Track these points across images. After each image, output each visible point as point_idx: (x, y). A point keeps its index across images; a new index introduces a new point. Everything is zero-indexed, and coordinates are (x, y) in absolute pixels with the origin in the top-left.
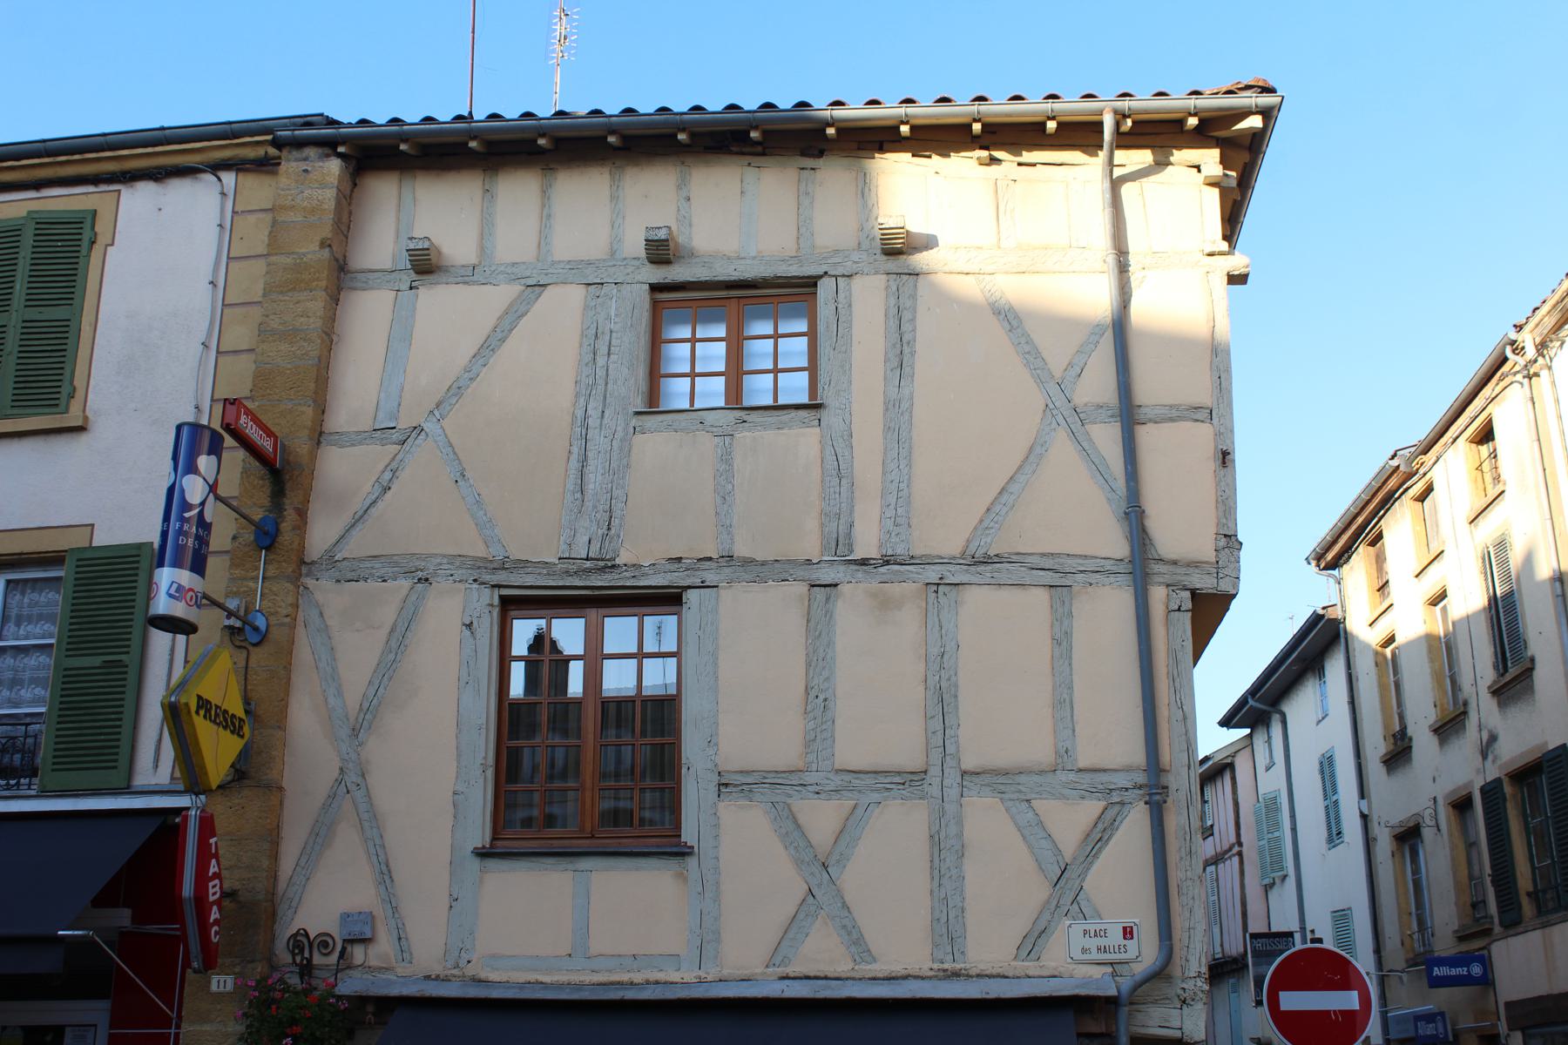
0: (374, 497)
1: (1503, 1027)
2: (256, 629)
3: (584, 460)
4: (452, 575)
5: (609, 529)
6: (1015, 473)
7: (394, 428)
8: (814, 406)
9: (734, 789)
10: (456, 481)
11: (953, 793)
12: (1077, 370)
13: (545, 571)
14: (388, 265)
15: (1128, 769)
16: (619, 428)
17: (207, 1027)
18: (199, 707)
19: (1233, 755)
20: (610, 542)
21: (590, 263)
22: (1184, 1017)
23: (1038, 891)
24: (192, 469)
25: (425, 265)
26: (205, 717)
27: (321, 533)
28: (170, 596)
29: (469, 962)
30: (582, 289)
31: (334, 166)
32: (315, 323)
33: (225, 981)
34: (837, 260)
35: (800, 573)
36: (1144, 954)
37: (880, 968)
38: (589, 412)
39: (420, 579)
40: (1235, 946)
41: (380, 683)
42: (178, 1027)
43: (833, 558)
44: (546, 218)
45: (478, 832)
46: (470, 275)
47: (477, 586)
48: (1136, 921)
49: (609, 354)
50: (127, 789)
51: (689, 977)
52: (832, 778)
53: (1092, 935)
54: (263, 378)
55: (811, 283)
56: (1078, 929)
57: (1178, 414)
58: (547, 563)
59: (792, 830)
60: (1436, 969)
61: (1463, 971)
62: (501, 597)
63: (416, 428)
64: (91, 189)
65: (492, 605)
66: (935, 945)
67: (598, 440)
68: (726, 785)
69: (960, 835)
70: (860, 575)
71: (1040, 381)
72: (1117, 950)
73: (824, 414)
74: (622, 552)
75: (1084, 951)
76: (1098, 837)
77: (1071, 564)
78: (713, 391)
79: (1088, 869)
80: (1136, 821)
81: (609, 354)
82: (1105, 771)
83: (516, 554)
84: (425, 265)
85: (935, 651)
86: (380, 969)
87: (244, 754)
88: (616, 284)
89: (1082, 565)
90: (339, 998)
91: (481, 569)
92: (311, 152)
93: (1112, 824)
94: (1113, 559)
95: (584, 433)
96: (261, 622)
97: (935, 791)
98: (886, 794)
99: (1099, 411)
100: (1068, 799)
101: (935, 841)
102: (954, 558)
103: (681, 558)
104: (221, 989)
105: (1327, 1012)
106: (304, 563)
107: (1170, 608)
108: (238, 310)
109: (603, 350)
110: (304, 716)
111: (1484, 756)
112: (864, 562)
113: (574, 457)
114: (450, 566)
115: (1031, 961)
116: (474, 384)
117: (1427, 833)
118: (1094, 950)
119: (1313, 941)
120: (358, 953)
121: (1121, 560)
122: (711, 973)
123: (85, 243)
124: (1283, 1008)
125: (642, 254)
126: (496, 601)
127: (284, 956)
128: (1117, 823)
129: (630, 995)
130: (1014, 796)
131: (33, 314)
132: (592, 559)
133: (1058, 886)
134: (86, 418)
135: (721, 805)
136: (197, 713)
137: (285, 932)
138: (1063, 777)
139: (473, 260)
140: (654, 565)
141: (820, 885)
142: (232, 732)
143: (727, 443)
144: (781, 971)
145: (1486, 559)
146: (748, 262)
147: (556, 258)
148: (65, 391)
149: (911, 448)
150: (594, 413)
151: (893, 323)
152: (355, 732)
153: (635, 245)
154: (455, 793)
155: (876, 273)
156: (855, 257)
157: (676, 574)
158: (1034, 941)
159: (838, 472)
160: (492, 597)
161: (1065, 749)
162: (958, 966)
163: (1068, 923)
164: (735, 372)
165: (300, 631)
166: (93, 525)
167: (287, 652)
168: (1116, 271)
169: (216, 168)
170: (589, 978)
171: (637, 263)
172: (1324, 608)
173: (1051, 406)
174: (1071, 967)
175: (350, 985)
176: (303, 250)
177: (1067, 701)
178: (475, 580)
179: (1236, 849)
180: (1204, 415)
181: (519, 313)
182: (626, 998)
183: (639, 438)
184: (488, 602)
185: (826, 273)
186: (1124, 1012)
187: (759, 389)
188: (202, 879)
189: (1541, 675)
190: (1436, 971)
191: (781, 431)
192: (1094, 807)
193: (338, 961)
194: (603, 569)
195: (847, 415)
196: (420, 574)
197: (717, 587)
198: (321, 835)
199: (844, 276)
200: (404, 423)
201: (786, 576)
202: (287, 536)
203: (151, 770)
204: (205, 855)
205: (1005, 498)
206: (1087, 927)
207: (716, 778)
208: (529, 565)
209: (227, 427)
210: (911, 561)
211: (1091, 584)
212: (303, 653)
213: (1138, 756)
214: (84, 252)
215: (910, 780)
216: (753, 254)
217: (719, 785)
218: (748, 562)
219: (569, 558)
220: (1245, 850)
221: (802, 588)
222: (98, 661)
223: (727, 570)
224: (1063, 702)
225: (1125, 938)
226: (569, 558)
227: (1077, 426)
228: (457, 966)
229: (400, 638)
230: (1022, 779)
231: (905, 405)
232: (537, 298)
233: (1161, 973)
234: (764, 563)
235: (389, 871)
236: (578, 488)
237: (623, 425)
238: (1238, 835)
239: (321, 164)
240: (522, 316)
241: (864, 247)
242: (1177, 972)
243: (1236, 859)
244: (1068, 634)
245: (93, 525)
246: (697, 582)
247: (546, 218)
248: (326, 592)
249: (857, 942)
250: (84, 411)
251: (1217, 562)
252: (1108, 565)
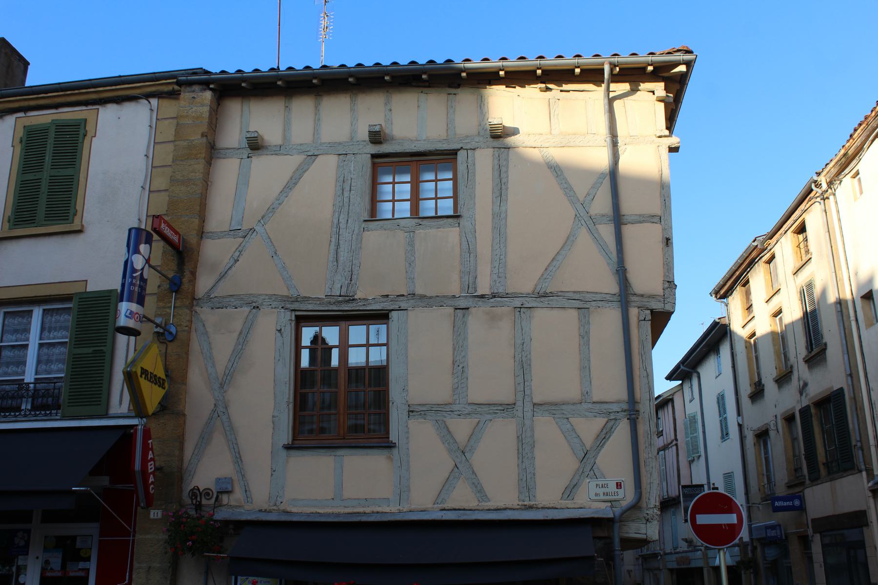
0: (230, 265)
1: (810, 532)
2: (171, 333)
3: (338, 245)
4: (271, 305)
5: (351, 280)
6: (560, 250)
7: (240, 229)
8: (456, 217)
9: (416, 414)
10: (272, 257)
11: (529, 414)
12: (591, 196)
13: (318, 302)
14: (236, 146)
15: (618, 402)
16: (356, 229)
17: (148, 536)
18: (142, 373)
19: (673, 395)
20: (352, 287)
21: (340, 144)
22: (648, 528)
23: (572, 464)
24: (137, 251)
25: (255, 145)
26: (145, 378)
27: (204, 284)
28: (127, 316)
29: (281, 503)
30: (336, 157)
31: (208, 95)
33: (157, 513)
34: (467, 141)
35: (450, 302)
36: (627, 496)
37: (492, 504)
38: (340, 220)
39: (254, 307)
40: (674, 492)
41: (234, 360)
42: (134, 536)
43: (466, 295)
44: (317, 121)
45: (286, 437)
46: (279, 150)
47: (284, 310)
48: (623, 479)
49: (350, 191)
50: (106, 415)
51: (394, 509)
52: (467, 407)
53: (601, 486)
54: (173, 204)
55: (454, 153)
56: (593, 484)
57: (644, 219)
58: (319, 298)
59: (446, 434)
60: (776, 502)
61: (789, 503)
62: (296, 316)
63: (251, 229)
64: (84, 108)
65: (291, 320)
66: (520, 493)
67: (345, 235)
68: (412, 411)
69: (533, 436)
70: (480, 303)
71: (572, 203)
72: (613, 494)
73: (461, 221)
74: (358, 292)
75: (596, 495)
76: (603, 437)
77: (589, 297)
78: (404, 209)
79: (598, 453)
80: (623, 429)
81: (350, 191)
82: (607, 403)
83: (304, 294)
84: (255, 145)
85: (519, 342)
86: (236, 507)
87: (165, 397)
88: (354, 154)
89: (594, 297)
90: (216, 521)
91: (286, 302)
92: (196, 88)
93: (611, 430)
94: (611, 294)
95: (338, 231)
96: (173, 330)
97: (521, 415)
98: (494, 415)
99: (603, 218)
100: (588, 417)
101: (520, 439)
102: (529, 294)
103: (388, 295)
104: (156, 517)
105: (721, 525)
106: (195, 299)
107: (641, 319)
108: (159, 169)
109: (348, 188)
110: (196, 378)
111: (801, 394)
112: (482, 297)
113: (333, 243)
114: (269, 300)
115: (568, 500)
116: (282, 206)
117: (772, 433)
118: (602, 494)
119: (714, 489)
120: (225, 499)
121: (615, 295)
122: (405, 507)
123: (81, 136)
124: (698, 523)
125: (367, 139)
126: (293, 318)
127: (187, 500)
128: (613, 429)
129: (364, 519)
130: (560, 416)
132: (343, 296)
133: (583, 462)
134: (82, 226)
135: (410, 422)
136: (141, 376)
137: (188, 487)
138: (585, 406)
139: (280, 142)
140: (374, 299)
141: (461, 462)
142: (159, 386)
143: (411, 236)
144: (441, 506)
145: (802, 293)
146: (422, 142)
147: (323, 141)
148: (72, 212)
149: (506, 237)
150: (343, 221)
151: (497, 173)
152: (222, 386)
153: (363, 134)
154: (273, 417)
155: (488, 148)
156: (477, 139)
157: (386, 303)
158: (571, 490)
159: (469, 250)
160: (291, 316)
161: (586, 391)
162: (532, 503)
163: (588, 480)
164: (416, 199)
165: (194, 335)
166: (86, 281)
167: (186, 345)
168: (611, 145)
169: (148, 96)
170: (342, 511)
171: (365, 143)
172: (719, 319)
173: (578, 215)
174: (590, 503)
175: (221, 515)
176: (193, 138)
177: (587, 367)
178: (282, 307)
179: (674, 443)
180: (656, 219)
181: (303, 170)
182: (362, 520)
183: (366, 233)
184: (289, 319)
185: (462, 148)
186: (617, 525)
187: (428, 208)
188: (145, 461)
189: (830, 352)
190: (777, 504)
191: (439, 229)
192: (601, 421)
193: (215, 503)
194: (348, 301)
195: (473, 221)
196: (254, 304)
197: (407, 310)
198: (205, 438)
199: (471, 149)
200: (245, 227)
201: (442, 304)
202: (186, 286)
203: (118, 406)
204: (146, 449)
205: (554, 263)
206: (598, 483)
207: (407, 408)
208: (310, 299)
209: (154, 230)
210: (507, 295)
211: (599, 307)
212: (195, 345)
213: (624, 395)
214: (81, 141)
215: (507, 408)
216: (424, 138)
217: (409, 411)
218: (422, 297)
219: (331, 296)
220: (679, 442)
221: (451, 310)
222: (90, 350)
223: (412, 301)
224: (585, 368)
225: (617, 488)
226: (331, 296)
227: (591, 226)
228: (275, 505)
230: (564, 407)
231: (503, 215)
232: (313, 162)
233: (635, 506)
234: (431, 298)
235: (240, 457)
236: (335, 260)
237: (358, 227)
238: (676, 435)
239: (201, 94)
240: (306, 171)
241: (481, 134)
242: (644, 505)
243: (674, 448)
244: (587, 333)
245: (86, 281)
246: (397, 307)
247: (317, 121)
248: (207, 315)
249: (479, 490)
250: (82, 222)
251: (664, 295)
252: (608, 297)
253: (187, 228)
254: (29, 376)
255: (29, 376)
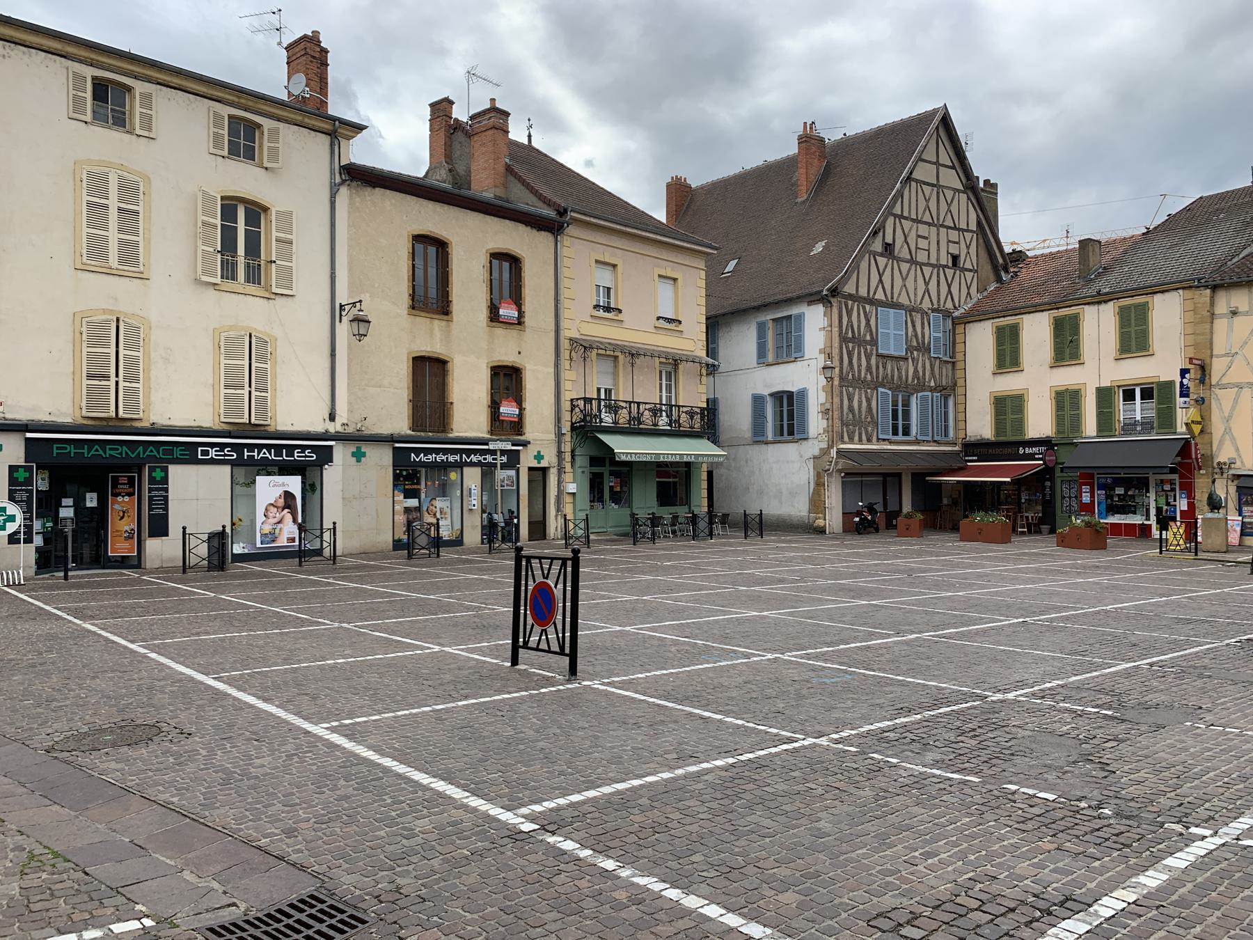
32: (1208, 331)
50: (1175, 433)
84: (1234, 313)
87: (1203, 427)
92: (1202, 288)
131: (1136, 328)
137: (1216, 462)
188: (1196, 454)
198: (1221, 443)
200: (1233, 352)
202: (1207, 380)
204: (1196, 450)
229: (1236, 401)
253: (1204, 355)
254: (1138, 418)
255: (1138, 418)
